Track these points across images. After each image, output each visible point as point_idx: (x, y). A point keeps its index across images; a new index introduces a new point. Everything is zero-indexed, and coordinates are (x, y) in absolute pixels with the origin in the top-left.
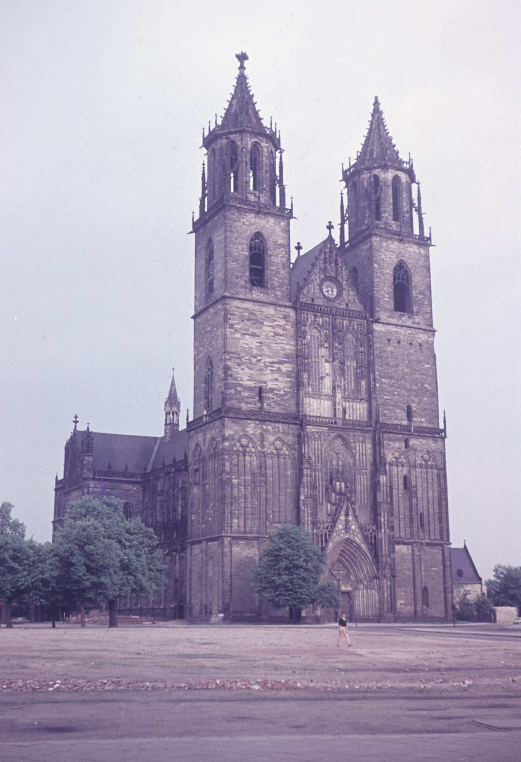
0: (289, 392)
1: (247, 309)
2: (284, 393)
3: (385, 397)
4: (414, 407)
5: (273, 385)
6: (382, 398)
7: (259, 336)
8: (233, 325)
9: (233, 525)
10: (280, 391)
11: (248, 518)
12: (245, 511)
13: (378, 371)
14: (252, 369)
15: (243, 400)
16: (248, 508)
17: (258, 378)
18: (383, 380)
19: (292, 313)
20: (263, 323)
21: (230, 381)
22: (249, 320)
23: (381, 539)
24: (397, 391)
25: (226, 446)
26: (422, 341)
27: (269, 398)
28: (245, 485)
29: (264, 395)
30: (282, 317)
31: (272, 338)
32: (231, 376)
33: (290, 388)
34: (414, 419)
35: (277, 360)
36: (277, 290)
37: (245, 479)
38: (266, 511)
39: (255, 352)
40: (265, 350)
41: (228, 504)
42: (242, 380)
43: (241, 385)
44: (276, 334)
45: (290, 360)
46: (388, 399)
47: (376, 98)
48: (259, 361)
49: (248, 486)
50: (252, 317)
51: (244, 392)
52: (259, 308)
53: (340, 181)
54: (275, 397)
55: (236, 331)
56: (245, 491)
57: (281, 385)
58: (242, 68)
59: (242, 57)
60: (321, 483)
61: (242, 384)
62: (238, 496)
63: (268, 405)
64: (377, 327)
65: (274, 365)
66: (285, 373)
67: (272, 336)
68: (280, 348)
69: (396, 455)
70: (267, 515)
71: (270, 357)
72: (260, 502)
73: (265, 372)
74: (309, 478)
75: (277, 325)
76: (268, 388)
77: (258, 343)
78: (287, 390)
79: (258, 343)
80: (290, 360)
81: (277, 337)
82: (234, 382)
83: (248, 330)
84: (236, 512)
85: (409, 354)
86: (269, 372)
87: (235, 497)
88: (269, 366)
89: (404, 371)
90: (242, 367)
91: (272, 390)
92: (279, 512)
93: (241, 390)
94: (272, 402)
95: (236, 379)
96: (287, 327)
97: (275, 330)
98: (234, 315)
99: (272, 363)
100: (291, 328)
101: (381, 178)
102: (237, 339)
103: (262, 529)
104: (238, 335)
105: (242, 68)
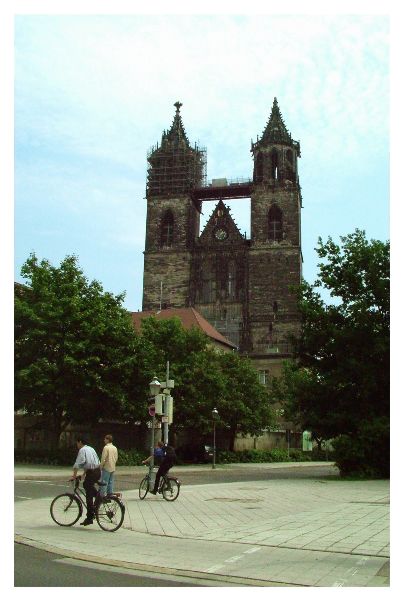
1: (157, 259)
2: (181, 305)
3: (256, 298)
4: (279, 302)
5: (173, 301)
6: (254, 299)
7: (165, 273)
8: (149, 269)
18: (255, 287)
19: (189, 255)
22: (159, 264)
24: (265, 293)
26: (289, 256)
34: (279, 310)
35: (177, 286)
40: (170, 281)
43: (152, 304)
44: (177, 270)
45: (186, 284)
46: (258, 299)
47: (275, 98)
48: (165, 288)
50: (162, 262)
51: (154, 308)
52: (167, 256)
55: (151, 272)
57: (179, 301)
58: (178, 111)
59: (178, 105)
61: (153, 304)
64: (252, 253)
65: (175, 289)
67: (174, 271)
69: (262, 336)
71: (172, 284)
73: (168, 294)
75: (178, 264)
76: (170, 304)
77: (165, 277)
79: (165, 277)
80: (186, 284)
85: (277, 267)
89: (272, 279)
90: (154, 293)
93: (152, 307)
95: (149, 301)
101: (263, 153)
102: (151, 277)
104: (152, 275)
105: (178, 111)
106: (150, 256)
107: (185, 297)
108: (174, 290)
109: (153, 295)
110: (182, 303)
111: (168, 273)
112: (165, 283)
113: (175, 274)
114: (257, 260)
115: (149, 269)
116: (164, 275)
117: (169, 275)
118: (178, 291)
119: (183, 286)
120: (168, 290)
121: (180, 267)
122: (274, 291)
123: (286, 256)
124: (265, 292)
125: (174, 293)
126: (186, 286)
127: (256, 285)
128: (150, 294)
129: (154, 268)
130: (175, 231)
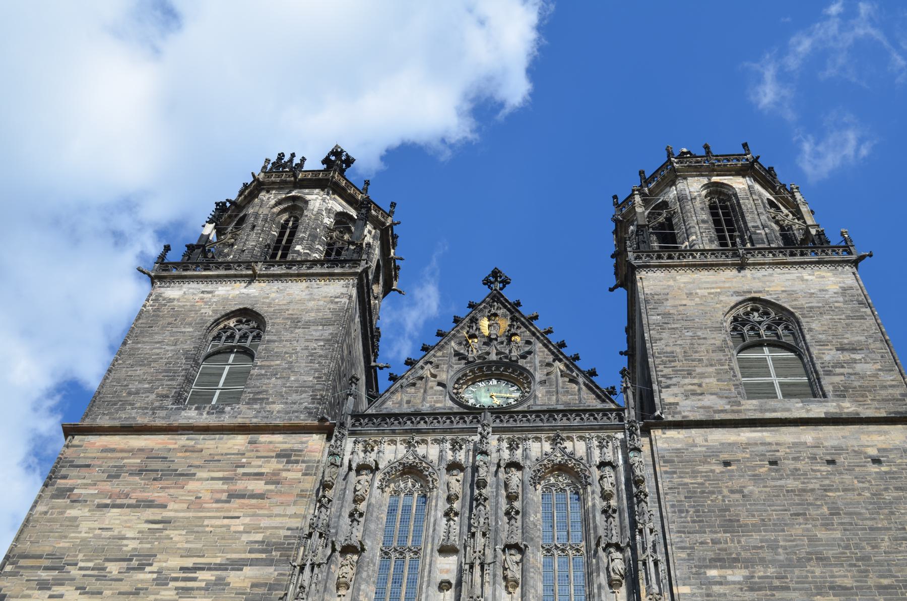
7: (164, 506)
8: (71, 490)
18: (713, 573)
20: (194, 474)
22: (140, 472)
30: (274, 454)
31: (215, 505)
35: (218, 561)
36: (274, 403)
39: (131, 545)
52: (192, 443)
53: (611, 290)
68: (241, 528)
71: (189, 553)
75: (244, 474)
81: (236, 503)
88: (176, 579)
89: (812, 540)
90: (57, 590)
97: (232, 487)
98: (88, 466)
99: (195, 569)
102: (75, 519)
104: (72, 513)
106: (97, 444)
109: (51, 597)
111: (171, 506)
112: (149, 546)
113: (218, 510)
114: (705, 462)
115: (71, 490)
116: (150, 514)
117: (181, 514)
119: (253, 563)
120: (155, 576)
121: (258, 486)
123: (873, 452)
126: (269, 562)
129: (107, 487)
130: (261, 367)
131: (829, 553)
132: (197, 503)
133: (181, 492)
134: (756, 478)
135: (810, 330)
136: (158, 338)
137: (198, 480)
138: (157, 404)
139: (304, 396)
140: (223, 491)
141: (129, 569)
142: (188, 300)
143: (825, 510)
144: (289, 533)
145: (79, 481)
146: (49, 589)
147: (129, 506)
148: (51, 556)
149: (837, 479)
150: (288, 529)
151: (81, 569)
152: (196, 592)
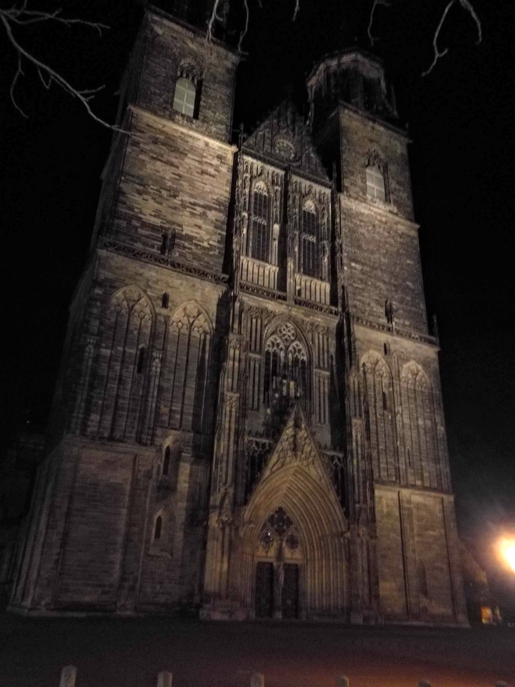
0: (218, 248)
2: (208, 246)
4: (395, 304)
7: (178, 167)
8: (138, 143)
9: (89, 423)
10: (203, 242)
11: (121, 416)
12: (116, 402)
13: (346, 252)
14: (161, 204)
15: (140, 239)
16: (124, 398)
17: (169, 217)
18: (353, 264)
20: (186, 155)
21: (122, 209)
23: (353, 476)
25: (98, 294)
27: (184, 247)
28: (123, 362)
29: (177, 241)
30: (216, 155)
32: (124, 203)
33: (219, 242)
37: (124, 352)
38: (157, 408)
39: (169, 184)
41: (84, 385)
42: (141, 212)
43: (139, 219)
44: (203, 172)
49: (130, 364)
51: (142, 229)
54: (193, 247)
55: (142, 151)
56: (121, 369)
60: (257, 379)
61: (141, 218)
62: (108, 375)
63: (181, 255)
65: (196, 207)
66: (212, 222)
68: (208, 190)
70: (158, 414)
71: (191, 196)
72: (148, 392)
73: (181, 213)
74: (236, 364)
75: (206, 162)
76: (184, 233)
77: (174, 174)
78: (215, 244)
79: (174, 174)
82: (128, 212)
83: (162, 156)
84: (100, 402)
86: (188, 214)
87: (103, 376)
89: (380, 260)
90: (145, 197)
91: (189, 238)
92: (182, 413)
93: (138, 225)
94: (188, 253)
95: (131, 209)
96: (221, 168)
99: (195, 204)
100: (228, 171)
103: (144, 437)
104: (142, 157)
107: (220, 234)
108: (195, 210)
109: (143, 199)
110: (211, 242)
111: (180, 168)
114: (354, 218)
115: (138, 143)
116: (173, 169)
117: (186, 175)
118: (203, 215)
119: (215, 209)
122: (385, 282)
124: (369, 278)
125: (193, 215)
127: (357, 262)
128: (133, 194)
129: (152, 147)
131: (384, 268)
132: (189, 170)
133: (182, 162)
134: (368, 230)
135: (390, 170)
136: (157, 60)
137: (189, 158)
138: (164, 105)
139: (223, 126)
140: (199, 168)
141: (170, 196)
142: (166, 39)
143: (385, 251)
144: (226, 199)
145: (141, 140)
146: (141, 195)
147: (164, 162)
148: (138, 177)
149: (389, 240)
150: (225, 197)
151: (152, 189)
152: (197, 216)
